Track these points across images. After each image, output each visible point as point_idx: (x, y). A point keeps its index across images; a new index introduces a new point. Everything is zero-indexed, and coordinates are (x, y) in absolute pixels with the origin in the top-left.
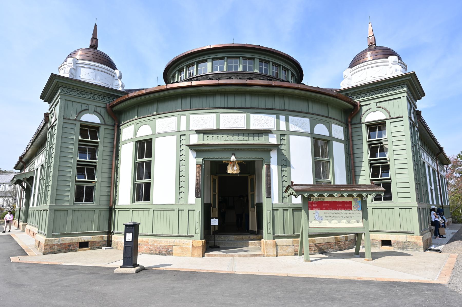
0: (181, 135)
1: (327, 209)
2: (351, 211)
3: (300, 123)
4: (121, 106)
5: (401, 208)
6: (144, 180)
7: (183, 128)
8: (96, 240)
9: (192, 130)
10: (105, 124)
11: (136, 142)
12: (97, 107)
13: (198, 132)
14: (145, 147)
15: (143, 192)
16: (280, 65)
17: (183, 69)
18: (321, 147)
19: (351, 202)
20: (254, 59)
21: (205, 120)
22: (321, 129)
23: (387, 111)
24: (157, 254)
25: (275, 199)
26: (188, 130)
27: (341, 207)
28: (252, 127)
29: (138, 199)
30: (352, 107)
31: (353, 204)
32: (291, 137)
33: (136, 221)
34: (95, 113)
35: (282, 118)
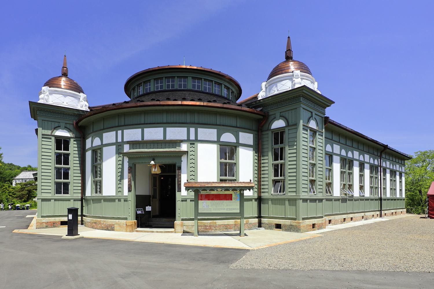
0: (119, 145)
1: (212, 199)
7: (120, 140)
12: (67, 124)
17: (135, 88)
18: (228, 152)
19: (232, 195)
27: (224, 198)
31: (233, 196)
34: (65, 128)
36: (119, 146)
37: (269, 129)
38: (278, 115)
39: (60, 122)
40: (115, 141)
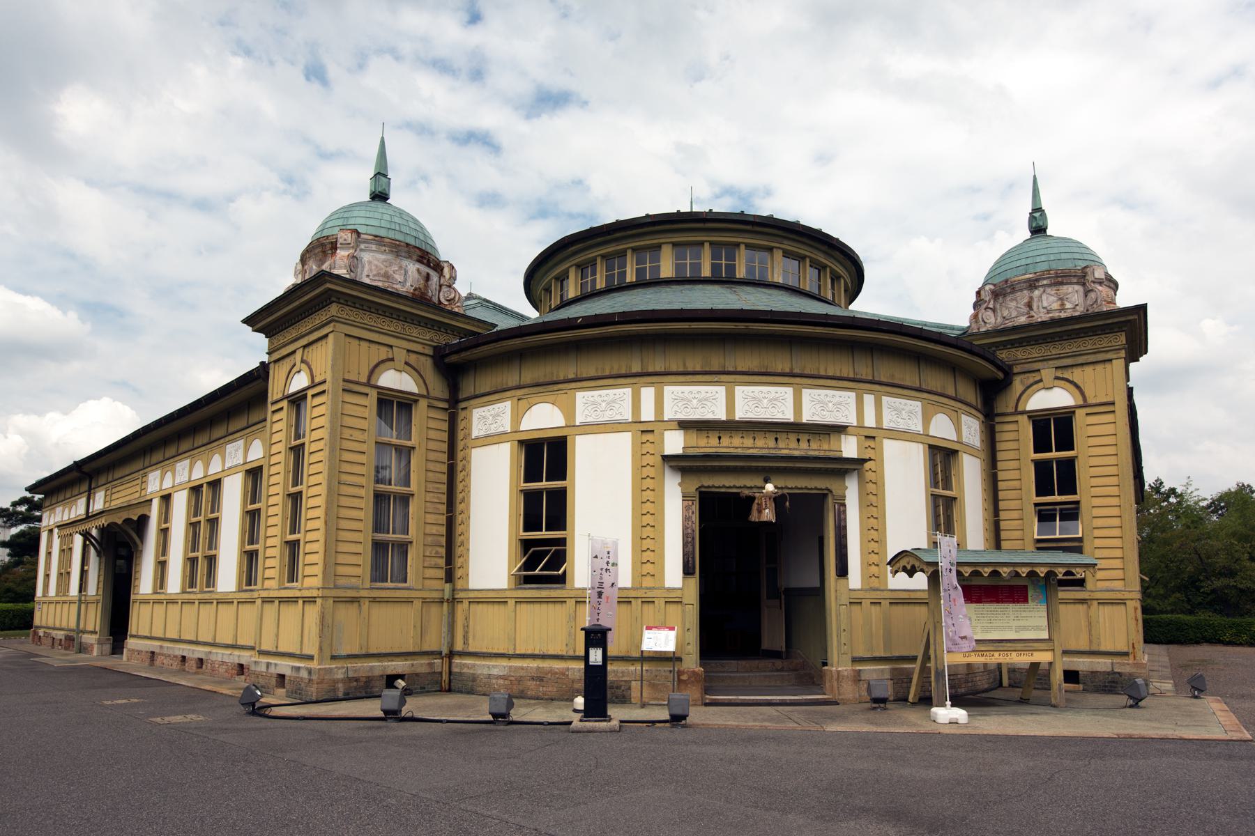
2: (1026, 606)
3: (902, 412)
4: (470, 355)
5: (1103, 603)
8: (419, 670)
10: (427, 397)
11: (521, 442)
13: (684, 425)
14: (545, 459)
15: (542, 560)
16: (825, 267)
19: (1026, 587)
20: (770, 249)
22: (942, 428)
23: (1077, 387)
25: (855, 578)
28: (806, 418)
30: (1001, 375)
32: (888, 444)
33: (605, 623)
34: (407, 368)
35: (869, 399)
36: (645, 431)
37: (1020, 409)
40: (628, 416)
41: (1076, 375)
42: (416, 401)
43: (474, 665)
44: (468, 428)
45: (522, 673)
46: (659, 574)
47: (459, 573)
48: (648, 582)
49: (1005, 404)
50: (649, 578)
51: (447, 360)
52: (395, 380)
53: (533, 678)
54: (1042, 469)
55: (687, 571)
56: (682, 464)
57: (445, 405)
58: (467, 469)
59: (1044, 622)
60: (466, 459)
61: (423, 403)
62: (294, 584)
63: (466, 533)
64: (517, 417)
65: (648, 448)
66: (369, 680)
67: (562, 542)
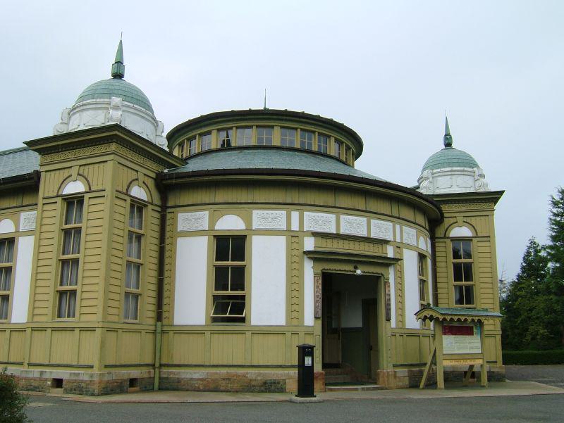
6: (229, 292)
9: (308, 232)
10: (152, 204)
11: (214, 236)
13: (315, 234)
14: (230, 250)
19: (472, 327)
20: (329, 137)
21: (324, 221)
24: (262, 391)
26: (301, 231)
28: (372, 236)
29: (59, 316)
36: (294, 237)
37: (447, 236)
38: (460, 219)
39: (137, 171)
41: (473, 221)
42: (146, 206)
43: (179, 373)
44: (175, 224)
45: (216, 377)
46: (301, 318)
47: (165, 315)
48: (295, 322)
49: (440, 232)
50: (295, 320)
51: (164, 182)
52: (138, 192)
53: (224, 379)
54: (457, 268)
55: (316, 318)
56: (315, 256)
57: (159, 209)
58: (174, 251)
59: (479, 345)
60: (174, 244)
61: (150, 207)
62: (62, 319)
63: (172, 291)
64: (212, 221)
65: (295, 245)
66: (122, 381)
67: (243, 297)
